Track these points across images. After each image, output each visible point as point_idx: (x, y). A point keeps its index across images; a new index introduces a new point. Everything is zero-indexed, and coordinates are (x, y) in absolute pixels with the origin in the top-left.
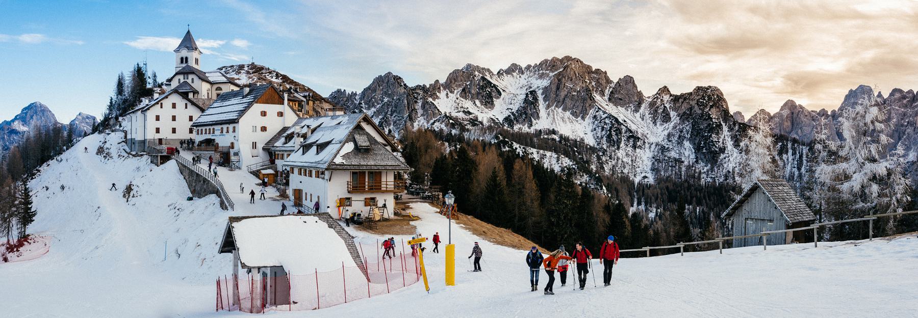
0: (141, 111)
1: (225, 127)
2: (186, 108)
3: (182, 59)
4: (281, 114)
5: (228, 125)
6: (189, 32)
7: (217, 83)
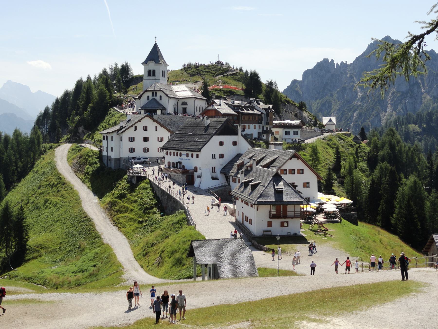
0: (116, 132)
1: (190, 153)
2: (156, 130)
3: (149, 72)
4: (235, 143)
5: (192, 153)
6: (156, 46)
7: (183, 98)
